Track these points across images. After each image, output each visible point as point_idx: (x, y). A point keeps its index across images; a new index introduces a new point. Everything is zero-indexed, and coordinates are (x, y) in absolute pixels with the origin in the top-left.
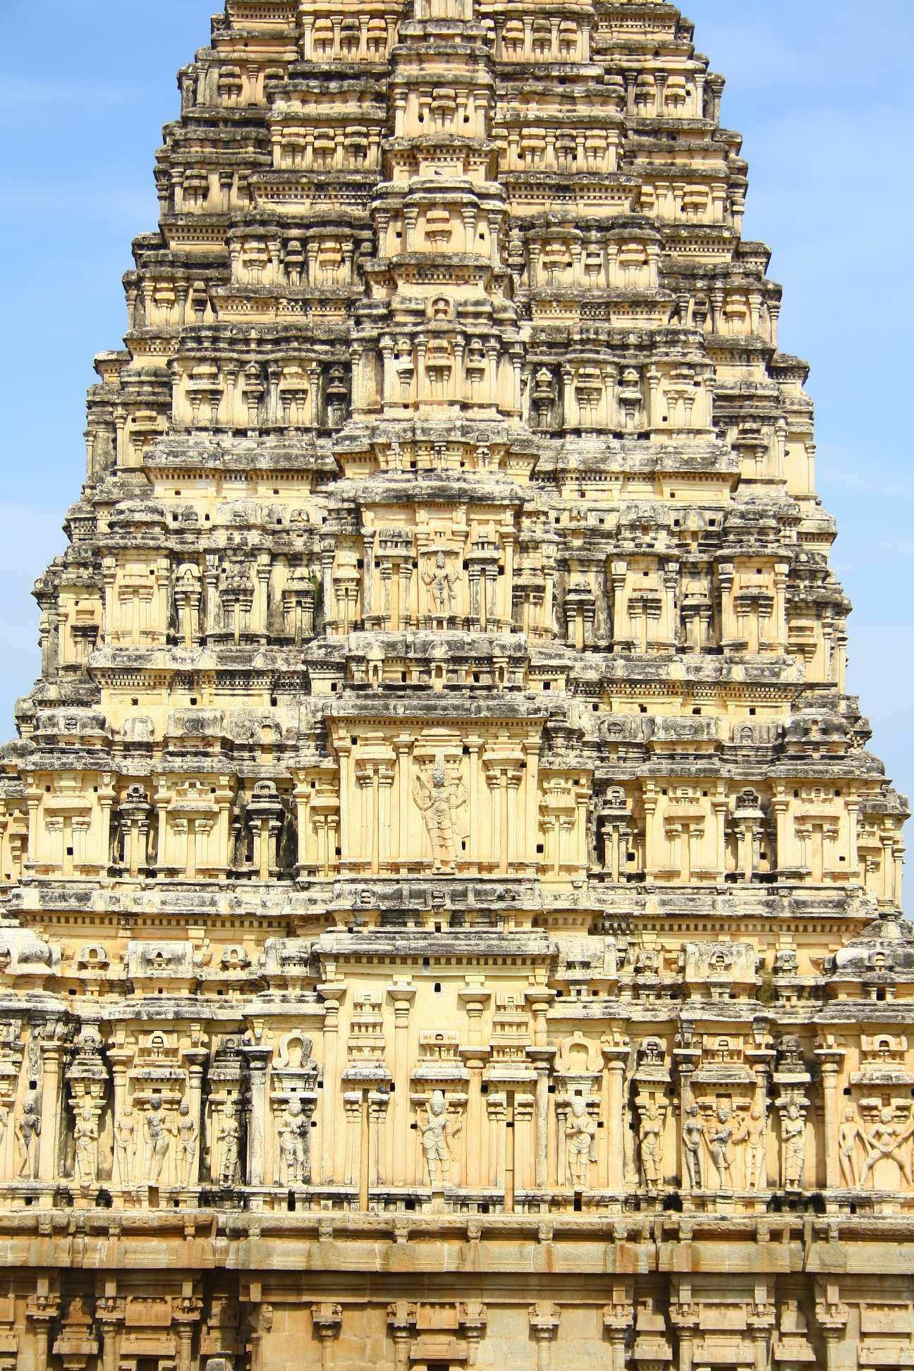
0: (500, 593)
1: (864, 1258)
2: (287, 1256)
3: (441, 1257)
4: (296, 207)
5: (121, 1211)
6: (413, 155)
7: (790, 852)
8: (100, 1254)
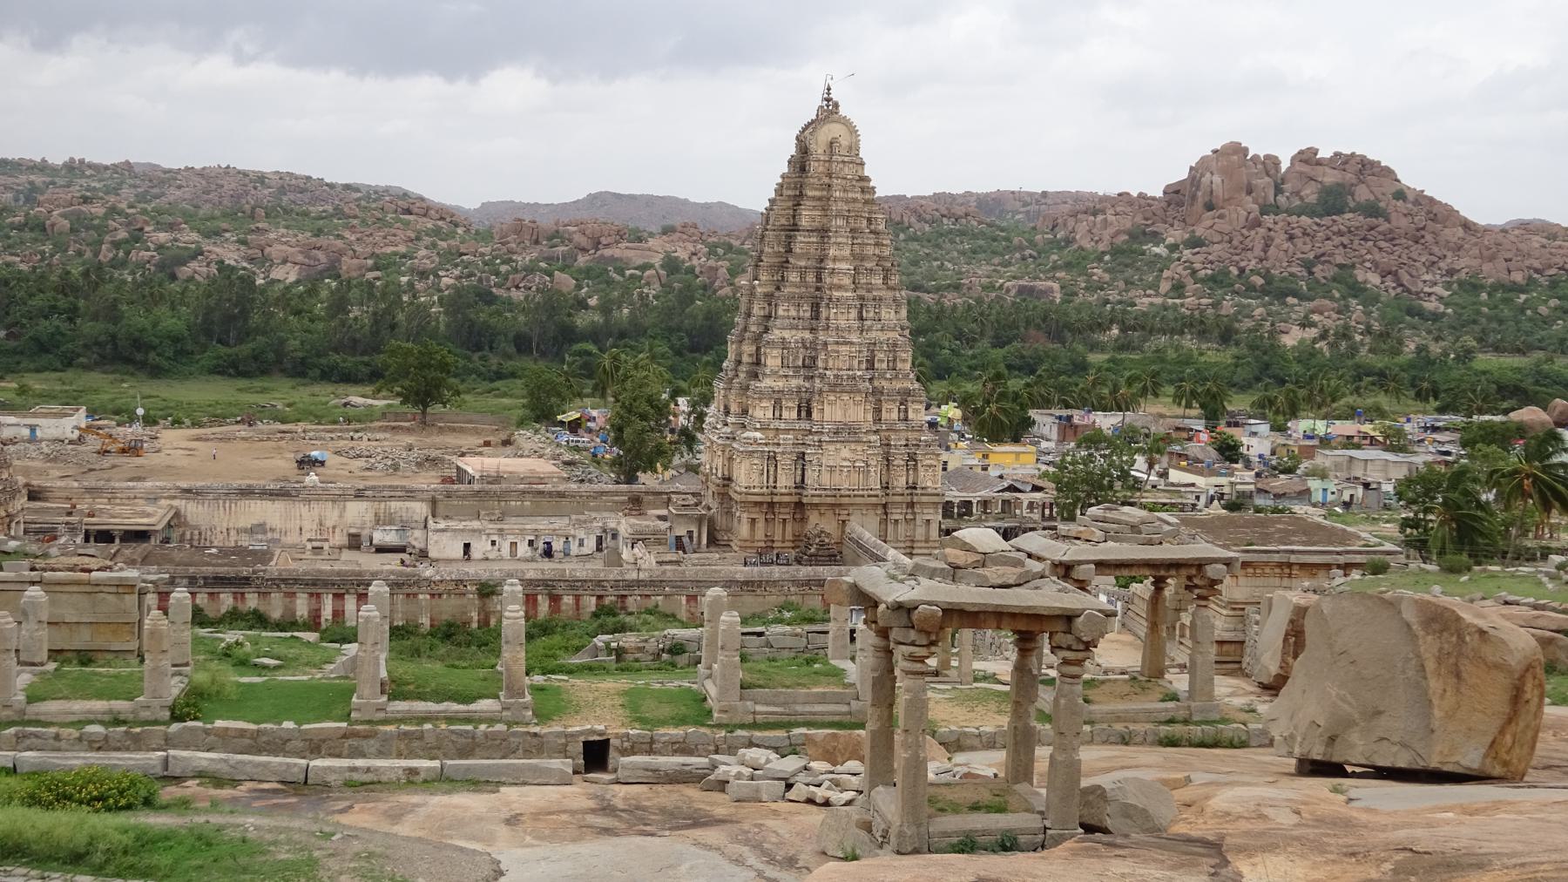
0: (856, 363)
1: (924, 499)
2: (816, 500)
3: (846, 500)
4: (803, 263)
5: (778, 490)
6: (835, 259)
7: (911, 415)
8: (776, 499)
